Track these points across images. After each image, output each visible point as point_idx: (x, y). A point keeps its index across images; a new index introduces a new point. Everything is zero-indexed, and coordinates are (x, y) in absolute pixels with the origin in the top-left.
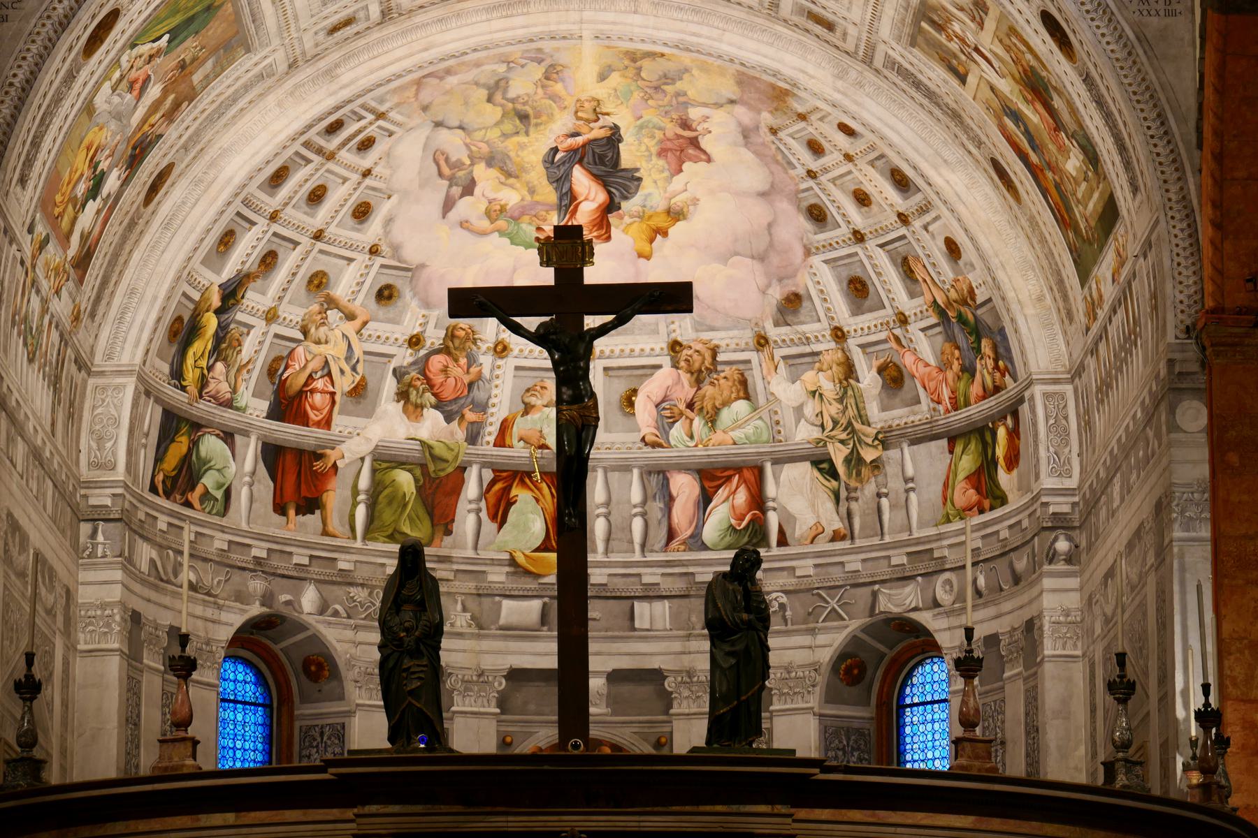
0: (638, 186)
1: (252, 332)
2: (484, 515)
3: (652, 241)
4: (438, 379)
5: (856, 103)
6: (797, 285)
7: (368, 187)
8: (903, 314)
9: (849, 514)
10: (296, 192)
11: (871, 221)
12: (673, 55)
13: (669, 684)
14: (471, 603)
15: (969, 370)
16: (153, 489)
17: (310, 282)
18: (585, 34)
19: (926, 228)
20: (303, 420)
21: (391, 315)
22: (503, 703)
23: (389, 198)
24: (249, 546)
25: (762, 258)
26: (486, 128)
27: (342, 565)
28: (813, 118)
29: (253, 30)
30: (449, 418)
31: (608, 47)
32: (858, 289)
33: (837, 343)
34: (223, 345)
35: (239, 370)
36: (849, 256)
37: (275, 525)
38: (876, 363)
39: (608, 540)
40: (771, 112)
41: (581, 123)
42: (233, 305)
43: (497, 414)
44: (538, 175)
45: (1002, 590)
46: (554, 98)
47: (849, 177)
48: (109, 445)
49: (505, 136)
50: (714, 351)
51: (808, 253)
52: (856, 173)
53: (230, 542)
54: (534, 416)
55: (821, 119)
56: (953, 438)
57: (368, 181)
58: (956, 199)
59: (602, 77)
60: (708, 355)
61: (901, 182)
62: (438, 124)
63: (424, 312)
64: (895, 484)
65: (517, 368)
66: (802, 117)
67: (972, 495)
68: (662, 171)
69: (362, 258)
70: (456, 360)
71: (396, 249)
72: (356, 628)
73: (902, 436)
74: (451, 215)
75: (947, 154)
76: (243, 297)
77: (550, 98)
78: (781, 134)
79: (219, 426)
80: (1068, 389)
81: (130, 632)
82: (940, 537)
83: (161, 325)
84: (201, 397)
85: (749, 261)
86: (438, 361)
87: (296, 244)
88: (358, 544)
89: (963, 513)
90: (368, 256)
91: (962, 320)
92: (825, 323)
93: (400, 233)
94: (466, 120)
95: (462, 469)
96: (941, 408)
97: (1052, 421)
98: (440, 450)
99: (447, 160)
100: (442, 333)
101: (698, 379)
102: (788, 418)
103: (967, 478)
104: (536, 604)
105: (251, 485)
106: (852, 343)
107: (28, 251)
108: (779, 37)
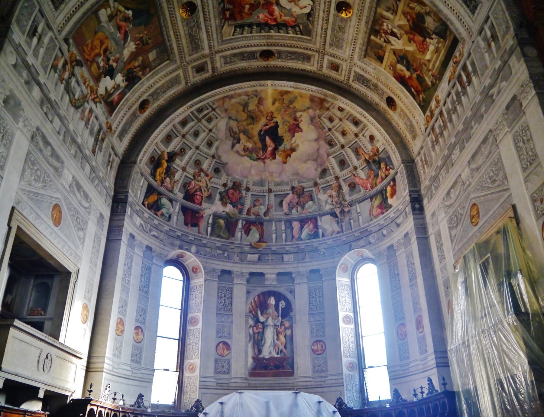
0: (283, 143)
2: (243, 233)
3: (286, 158)
4: (231, 196)
9: (342, 226)
13: (293, 275)
14: (239, 255)
16: (143, 204)
19: (363, 135)
20: (194, 202)
22: (248, 281)
24: (176, 232)
25: (315, 160)
26: (243, 121)
27: (203, 242)
29: (169, 47)
30: (234, 207)
31: (275, 90)
32: (343, 163)
34: (169, 172)
35: (175, 182)
37: (185, 229)
38: (348, 184)
39: (276, 238)
40: (319, 110)
43: (247, 206)
44: (256, 138)
45: (392, 231)
46: (261, 111)
48: (125, 182)
49: (248, 124)
50: (303, 188)
52: (343, 125)
53: (170, 229)
54: (256, 208)
55: (333, 108)
57: (211, 134)
60: (301, 190)
61: (356, 123)
64: (354, 215)
65: (252, 195)
67: (379, 211)
69: (210, 159)
70: (236, 191)
71: (219, 157)
72: (207, 259)
73: (356, 202)
74: (235, 149)
78: (322, 118)
79: (167, 196)
81: (129, 239)
82: (370, 225)
86: (231, 191)
87: (191, 149)
88: (208, 237)
89: (376, 217)
91: (374, 161)
93: (220, 152)
95: (237, 220)
96: (368, 191)
98: (231, 215)
99: (233, 131)
100: (232, 184)
101: (299, 197)
102: (323, 204)
103: (378, 207)
104: (257, 256)
105: (177, 216)
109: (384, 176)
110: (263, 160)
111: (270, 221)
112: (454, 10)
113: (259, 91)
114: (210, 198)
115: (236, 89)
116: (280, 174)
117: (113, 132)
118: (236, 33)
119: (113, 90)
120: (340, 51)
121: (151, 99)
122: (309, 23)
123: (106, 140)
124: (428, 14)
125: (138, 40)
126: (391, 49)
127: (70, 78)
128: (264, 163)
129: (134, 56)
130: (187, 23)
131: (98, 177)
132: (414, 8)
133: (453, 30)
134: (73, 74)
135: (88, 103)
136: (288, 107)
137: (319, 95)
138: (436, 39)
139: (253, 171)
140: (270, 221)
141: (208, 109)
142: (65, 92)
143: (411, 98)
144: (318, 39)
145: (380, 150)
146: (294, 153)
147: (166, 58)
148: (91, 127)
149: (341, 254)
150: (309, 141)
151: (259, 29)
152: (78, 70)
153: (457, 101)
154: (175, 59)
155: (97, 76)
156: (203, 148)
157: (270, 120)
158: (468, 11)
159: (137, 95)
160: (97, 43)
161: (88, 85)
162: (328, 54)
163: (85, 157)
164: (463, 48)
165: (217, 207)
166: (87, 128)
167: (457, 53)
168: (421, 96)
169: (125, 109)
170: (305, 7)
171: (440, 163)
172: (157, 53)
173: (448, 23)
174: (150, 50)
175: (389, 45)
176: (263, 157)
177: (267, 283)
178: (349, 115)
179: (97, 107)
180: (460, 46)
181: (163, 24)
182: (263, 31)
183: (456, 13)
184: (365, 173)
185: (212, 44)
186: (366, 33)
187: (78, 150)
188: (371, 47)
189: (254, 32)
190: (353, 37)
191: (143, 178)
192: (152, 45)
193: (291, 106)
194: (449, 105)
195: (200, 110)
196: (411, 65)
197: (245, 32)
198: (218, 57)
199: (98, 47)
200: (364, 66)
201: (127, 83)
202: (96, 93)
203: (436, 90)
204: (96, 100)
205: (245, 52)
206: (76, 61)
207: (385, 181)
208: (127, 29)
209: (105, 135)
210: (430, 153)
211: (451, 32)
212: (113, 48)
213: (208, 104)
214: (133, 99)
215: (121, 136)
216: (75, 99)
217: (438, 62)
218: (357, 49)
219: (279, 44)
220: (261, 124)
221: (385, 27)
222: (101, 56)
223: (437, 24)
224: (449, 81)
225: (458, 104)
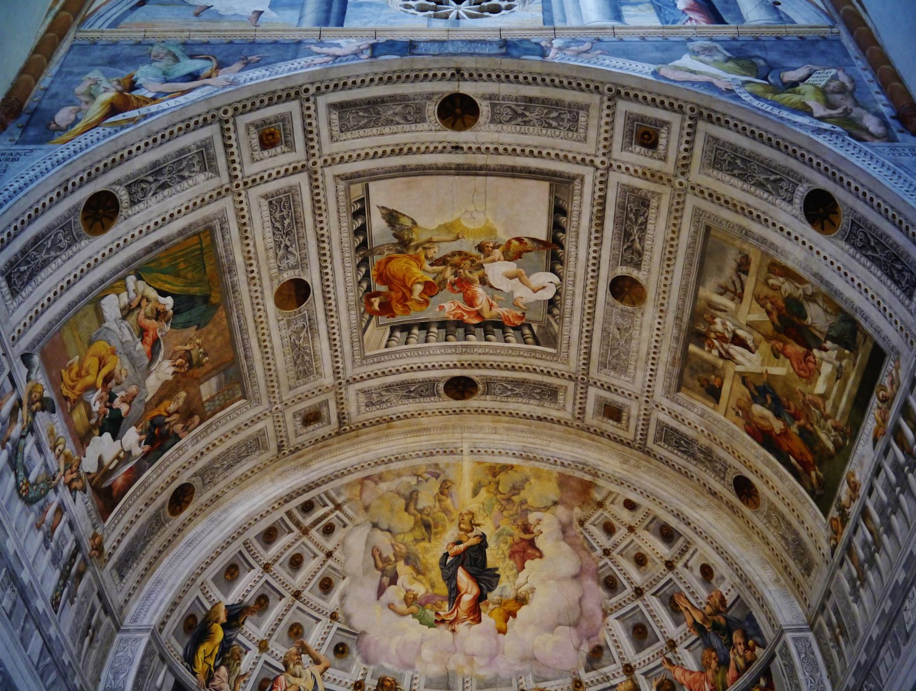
1: (249, 653)
3: (506, 620)
5: (637, 476)
6: (599, 640)
7: (330, 566)
8: (672, 641)
10: (282, 553)
11: (647, 577)
12: (519, 466)
17: (291, 629)
18: (466, 447)
19: (686, 566)
21: (343, 665)
23: (344, 578)
25: (575, 625)
26: (404, 533)
28: (607, 503)
29: (246, 370)
31: (479, 463)
33: (627, 675)
35: (239, 678)
36: (633, 609)
38: (655, 684)
40: (580, 506)
41: (462, 533)
42: (236, 626)
44: (436, 574)
46: (446, 511)
47: (632, 546)
48: (122, 676)
49: (416, 541)
51: (605, 614)
52: (637, 541)
55: (612, 503)
57: (330, 562)
58: (708, 525)
59: (475, 493)
62: (375, 526)
63: (364, 666)
66: (600, 505)
68: (512, 569)
69: (326, 620)
71: (348, 618)
74: (383, 598)
75: (699, 502)
76: (243, 623)
77: (444, 512)
78: (587, 525)
80: (810, 635)
83: (176, 612)
84: (208, 687)
85: (567, 628)
87: (282, 596)
90: (329, 620)
91: (716, 627)
92: (619, 664)
93: (351, 606)
94: (392, 525)
97: (803, 656)
99: (380, 555)
100: (376, 683)
106: (637, 673)
108: (585, 444)
109: (741, 662)
112: (866, 291)
113: (441, 466)
115: (390, 461)
116: (492, 657)
117: (106, 557)
118: (393, 343)
119: (116, 461)
120: (623, 377)
121: (197, 483)
122: (552, 320)
123: (88, 575)
124: (811, 298)
125: (180, 357)
126: (735, 372)
127: (23, 437)
128: (453, 631)
129: (167, 391)
130: (289, 323)
131: (57, 664)
132: (780, 287)
133: (870, 331)
134: (31, 429)
135: (56, 491)
136: (509, 500)
137: (578, 474)
138: (834, 349)
139: (426, 653)
141: (325, 505)
142: (9, 468)
143: (792, 478)
144: (573, 351)
145: (729, 600)
146: (524, 608)
147: (240, 395)
148: (57, 544)
150: (559, 580)
151: (443, 332)
152: (42, 419)
153: (897, 485)
154: (257, 395)
155: (83, 432)
156: (311, 596)
157: (467, 531)
158: (898, 292)
159: (167, 473)
160: (92, 363)
161: (61, 452)
162: (595, 383)
163: (32, 614)
164: (897, 368)
166: (47, 548)
167: (885, 380)
168: (813, 474)
169: (140, 503)
170: (544, 288)
171: (875, 632)
172: (219, 384)
173: (858, 317)
174: (207, 376)
175: (730, 364)
176: (451, 618)
178: (650, 518)
179: (75, 500)
180: (889, 365)
181: (237, 325)
182: (451, 337)
183: (873, 297)
184: (695, 658)
185: (339, 365)
186: (677, 339)
187: (20, 601)
188: (692, 368)
189: (431, 338)
190: (649, 348)
191: (165, 667)
192: (209, 367)
193: (514, 498)
194: (881, 493)
195: (307, 507)
196: (784, 407)
197: (411, 340)
198: (353, 389)
199: (93, 371)
200: (678, 409)
201: (147, 447)
202: (77, 471)
203: (846, 461)
204: (75, 484)
205: (413, 382)
206: (42, 400)
207: (746, 676)
208: (159, 335)
209: (86, 564)
210: (848, 606)
211: (866, 336)
212: (123, 372)
213: (326, 493)
214: (159, 482)
215: (122, 567)
216: (28, 482)
217: (844, 399)
218: (661, 373)
219: (488, 365)
221: (719, 327)
222: (97, 389)
223: (832, 319)
224: (875, 441)
225: (902, 492)
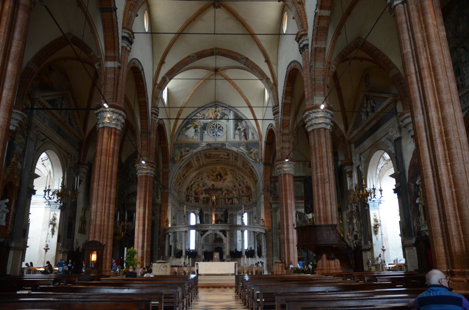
15: (248, 191)
32: (240, 185)
34: (191, 190)
44: (215, 176)
56: (247, 196)
101: (228, 192)
107: (175, 183)
110: (217, 181)
111: (219, 199)
114: (202, 193)
140: (219, 199)
149: (239, 210)
165: (204, 195)
177: (218, 217)
195: (199, 173)
220: (216, 173)
